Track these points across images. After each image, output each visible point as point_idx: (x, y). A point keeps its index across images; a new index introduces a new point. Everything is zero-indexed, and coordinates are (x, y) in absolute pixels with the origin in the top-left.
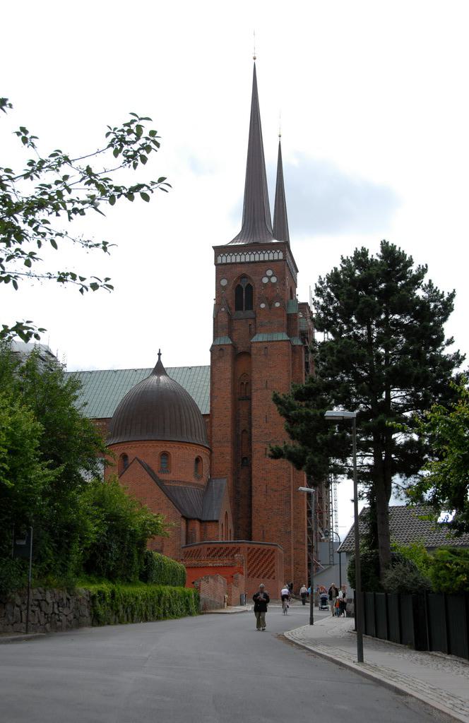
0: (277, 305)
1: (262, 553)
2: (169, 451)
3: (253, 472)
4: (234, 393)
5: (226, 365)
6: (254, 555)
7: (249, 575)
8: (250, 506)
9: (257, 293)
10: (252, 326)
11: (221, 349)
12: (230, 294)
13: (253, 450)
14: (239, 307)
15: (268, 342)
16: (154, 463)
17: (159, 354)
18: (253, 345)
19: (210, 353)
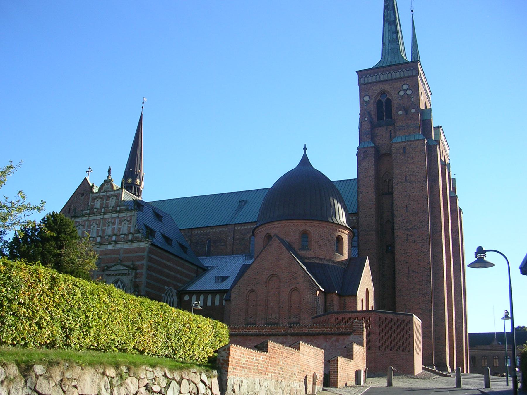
0: (413, 111)
1: (395, 323)
2: (309, 230)
3: (396, 257)
4: (377, 187)
5: (370, 164)
6: (386, 326)
7: (380, 347)
8: (394, 287)
9: (395, 104)
10: (392, 131)
11: (365, 152)
12: (372, 108)
13: (395, 236)
14: (380, 117)
15: (405, 142)
16: (295, 240)
17: (305, 149)
18: (393, 146)
19: (356, 158)
